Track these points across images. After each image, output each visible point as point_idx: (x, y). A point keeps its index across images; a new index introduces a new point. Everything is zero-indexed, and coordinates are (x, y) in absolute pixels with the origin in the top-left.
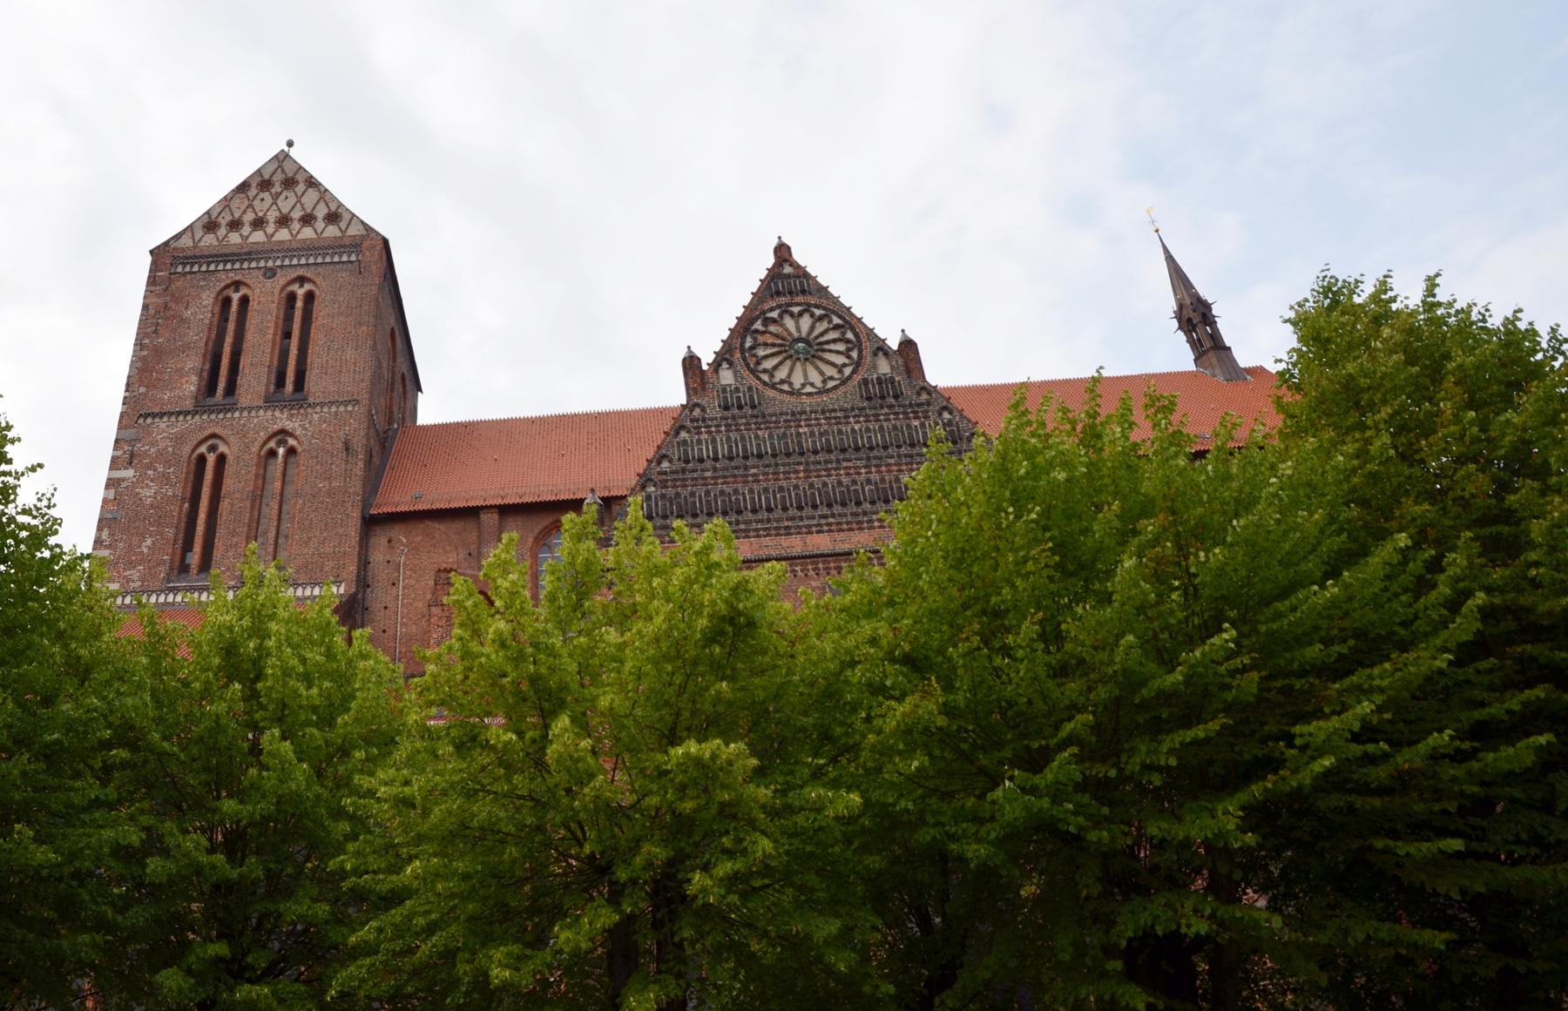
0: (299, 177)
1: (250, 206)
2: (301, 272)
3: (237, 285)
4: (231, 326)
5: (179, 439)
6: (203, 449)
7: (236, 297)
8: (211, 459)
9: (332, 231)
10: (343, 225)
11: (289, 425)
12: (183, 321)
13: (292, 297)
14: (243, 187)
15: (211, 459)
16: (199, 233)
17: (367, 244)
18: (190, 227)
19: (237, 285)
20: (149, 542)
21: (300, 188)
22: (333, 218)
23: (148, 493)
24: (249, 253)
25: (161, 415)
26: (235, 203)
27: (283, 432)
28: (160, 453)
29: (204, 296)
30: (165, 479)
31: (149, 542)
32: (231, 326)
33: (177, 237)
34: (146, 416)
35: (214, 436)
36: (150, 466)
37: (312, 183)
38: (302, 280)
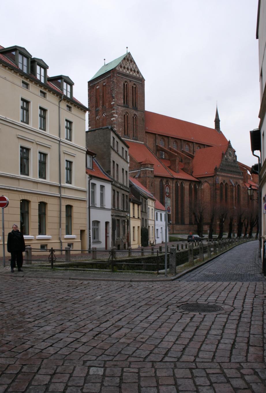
0: (132, 60)
1: (126, 64)
2: (134, 83)
3: (126, 82)
4: (125, 90)
5: (122, 111)
6: (125, 114)
7: (126, 84)
8: (126, 116)
9: (138, 75)
10: (139, 74)
11: (136, 113)
12: (120, 87)
13: (133, 87)
14: (124, 59)
15: (126, 116)
16: (119, 68)
17: (143, 80)
18: (118, 65)
19: (126, 82)
20: (121, 129)
21: (133, 63)
22: (138, 72)
23: (120, 120)
24: (127, 75)
25: (119, 106)
26: (124, 62)
27: (135, 114)
28: (120, 113)
29: (122, 82)
30: (121, 118)
31: (121, 129)
32: (125, 90)
33: (116, 67)
34: (117, 105)
35: (126, 112)
36: (119, 115)
37: (135, 63)
38: (134, 84)
